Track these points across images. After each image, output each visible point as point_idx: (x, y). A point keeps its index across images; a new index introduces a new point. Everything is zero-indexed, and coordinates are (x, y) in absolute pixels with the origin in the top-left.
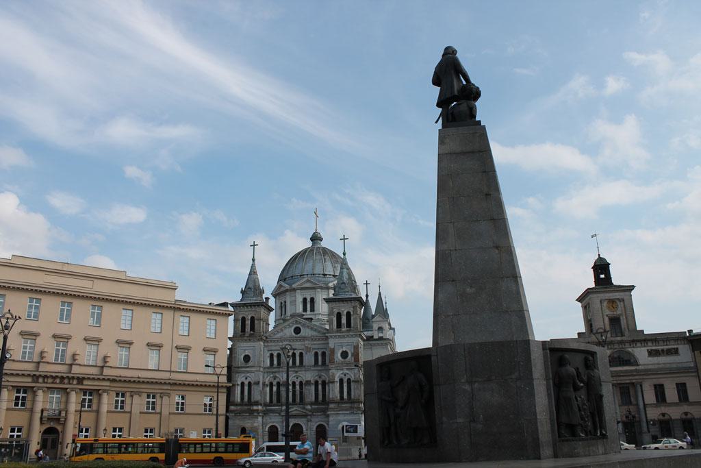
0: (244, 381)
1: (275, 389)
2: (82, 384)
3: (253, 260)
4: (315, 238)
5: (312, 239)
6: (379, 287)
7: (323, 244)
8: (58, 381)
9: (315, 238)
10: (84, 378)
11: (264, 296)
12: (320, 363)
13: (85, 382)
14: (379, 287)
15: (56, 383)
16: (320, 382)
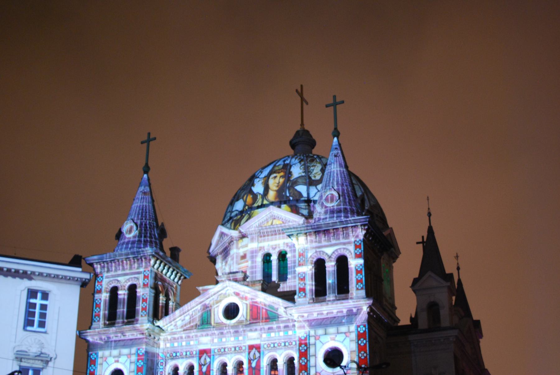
3: (146, 170)
6: (429, 215)
14: (429, 215)
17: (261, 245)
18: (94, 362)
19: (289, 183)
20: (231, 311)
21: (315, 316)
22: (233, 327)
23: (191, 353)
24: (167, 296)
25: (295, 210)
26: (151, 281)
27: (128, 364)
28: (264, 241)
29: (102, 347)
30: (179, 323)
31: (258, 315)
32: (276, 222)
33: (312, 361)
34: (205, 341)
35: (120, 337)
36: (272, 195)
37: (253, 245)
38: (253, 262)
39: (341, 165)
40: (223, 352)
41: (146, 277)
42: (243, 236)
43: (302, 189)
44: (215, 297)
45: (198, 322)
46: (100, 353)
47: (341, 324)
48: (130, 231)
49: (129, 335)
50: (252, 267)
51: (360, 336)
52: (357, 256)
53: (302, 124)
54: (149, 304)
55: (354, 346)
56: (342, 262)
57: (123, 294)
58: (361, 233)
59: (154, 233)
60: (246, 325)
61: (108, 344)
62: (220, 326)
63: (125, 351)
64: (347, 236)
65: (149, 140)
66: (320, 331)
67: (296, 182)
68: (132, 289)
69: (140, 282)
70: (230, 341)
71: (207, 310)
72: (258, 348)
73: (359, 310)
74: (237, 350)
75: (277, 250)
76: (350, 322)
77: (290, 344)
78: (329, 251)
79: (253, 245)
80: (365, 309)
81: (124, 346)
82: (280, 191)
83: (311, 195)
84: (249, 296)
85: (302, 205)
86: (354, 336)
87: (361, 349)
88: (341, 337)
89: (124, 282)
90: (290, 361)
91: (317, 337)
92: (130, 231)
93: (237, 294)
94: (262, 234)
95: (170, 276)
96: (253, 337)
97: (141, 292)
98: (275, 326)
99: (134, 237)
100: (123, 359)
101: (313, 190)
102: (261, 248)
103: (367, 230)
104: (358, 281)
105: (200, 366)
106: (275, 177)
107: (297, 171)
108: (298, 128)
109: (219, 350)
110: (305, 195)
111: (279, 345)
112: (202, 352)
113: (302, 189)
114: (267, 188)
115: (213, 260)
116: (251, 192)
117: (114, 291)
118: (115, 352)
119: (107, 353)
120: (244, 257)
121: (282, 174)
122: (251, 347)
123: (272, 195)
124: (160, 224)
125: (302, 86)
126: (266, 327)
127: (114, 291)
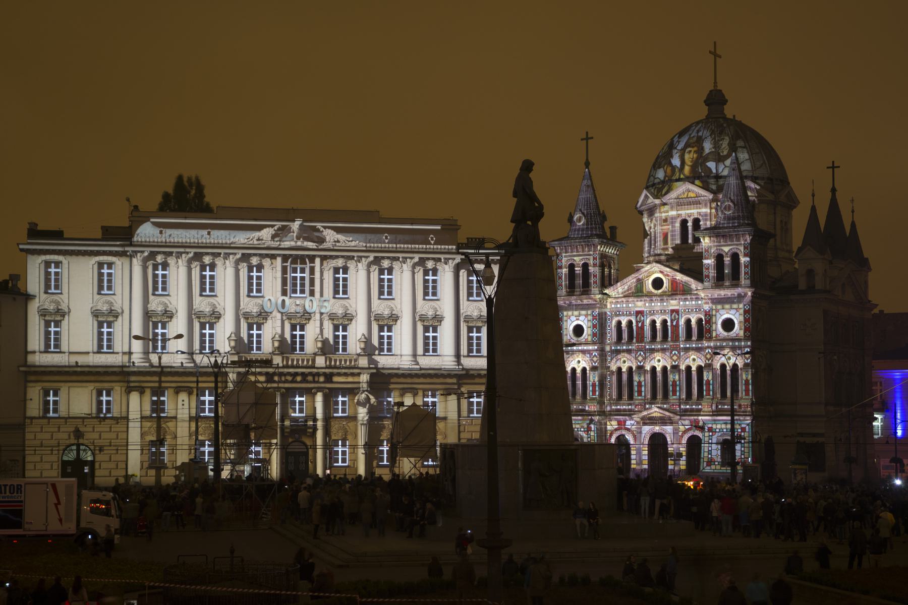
0: (576, 366)
1: (625, 377)
2: (332, 382)
3: (587, 164)
4: (716, 100)
5: (707, 102)
7: (729, 111)
8: (299, 378)
9: (716, 100)
10: (332, 375)
11: (607, 225)
13: (335, 379)
15: (296, 382)
17: (680, 212)
18: (561, 319)
19: (701, 160)
20: (658, 283)
21: (716, 296)
22: (660, 296)
23: (630, 313)
24: (610, 268)
25: (706, 187)
26: (598, 262)
27: (586, 321)
28: (682, 209)
29: (567, 309)
30: (620, 290)
31: (678, 290)
32: (692, 195)
33: (714, 326)
34: (640, 305)
35: (579, 302)
36: (687, 169)
37: (673, 213)
38: (673, 227)
39: (737, 179)
40: (652, 313)
41: (595, 259)
42: (665, 204)
43: (711, 165)
44: (646, 274)
45: (633, 290)
46: (565, 313)
47: (733, 303)
48: (580, 220)
49: (585, 302)
50: (672, 231)
51: (745, 312)
52: (745, 255)
53: (715, 82)
54: (598, 279)
55: (742, 318)
56: (735, 257)
57: (578, 270)
58: (748, 239)
59: (600, 228)
60: (669, 296)
61: (570, 307)
62: (650, 295)
63: (583, 312)
64: (738, 240)
65: (587, 139)
66: (719, 307)
67: (707, 159)
68: (585, 266)
69: (591, 262)
70: (657, 305)
71: (640, 282)
72: (677, 311)
73: (746, 295)
74: (663, 312)
75: (692, 218)
76: (739, 302)
77: (700, 310)
78: (726, 249)
79: (673, 213)
80: (750, 294)
81: (583, 309)
82: (693, 168)
83: (720, 170)
85: (712, 181)
86: (742, 311)
87: (746, 320)
88: (733, 312)
89: (578, 260)
90: (699, 321)
91: (717, 311)
92: (580, 220)
93: (661, 272)
94: (681, 203)
95: (611, 251)
96: (673, 304)
97: (591, 269)
98: (689, 297)
100: (582, 318)
101: (721, 167)
102: (679, 215)
103: (754, 236)
104: (745, 273)
105: (637, 322)
106: (690, 152)
107: (708, 146)
109: (650, 312)
110: (714, 171)
111: (692, 310)
112: (638, 313)
113: (711, 165)
114: (683, 163)
115: (641, 213)
116: (670, 164)
117: (572, 267)
118: (576, 313)
119: (570, 313)
120: (665, 220)
121: (695, 149)
122: (672, 311)
123: (687, 169)
125: (715, 43)
126: (683, 297)
127: (572, 267)
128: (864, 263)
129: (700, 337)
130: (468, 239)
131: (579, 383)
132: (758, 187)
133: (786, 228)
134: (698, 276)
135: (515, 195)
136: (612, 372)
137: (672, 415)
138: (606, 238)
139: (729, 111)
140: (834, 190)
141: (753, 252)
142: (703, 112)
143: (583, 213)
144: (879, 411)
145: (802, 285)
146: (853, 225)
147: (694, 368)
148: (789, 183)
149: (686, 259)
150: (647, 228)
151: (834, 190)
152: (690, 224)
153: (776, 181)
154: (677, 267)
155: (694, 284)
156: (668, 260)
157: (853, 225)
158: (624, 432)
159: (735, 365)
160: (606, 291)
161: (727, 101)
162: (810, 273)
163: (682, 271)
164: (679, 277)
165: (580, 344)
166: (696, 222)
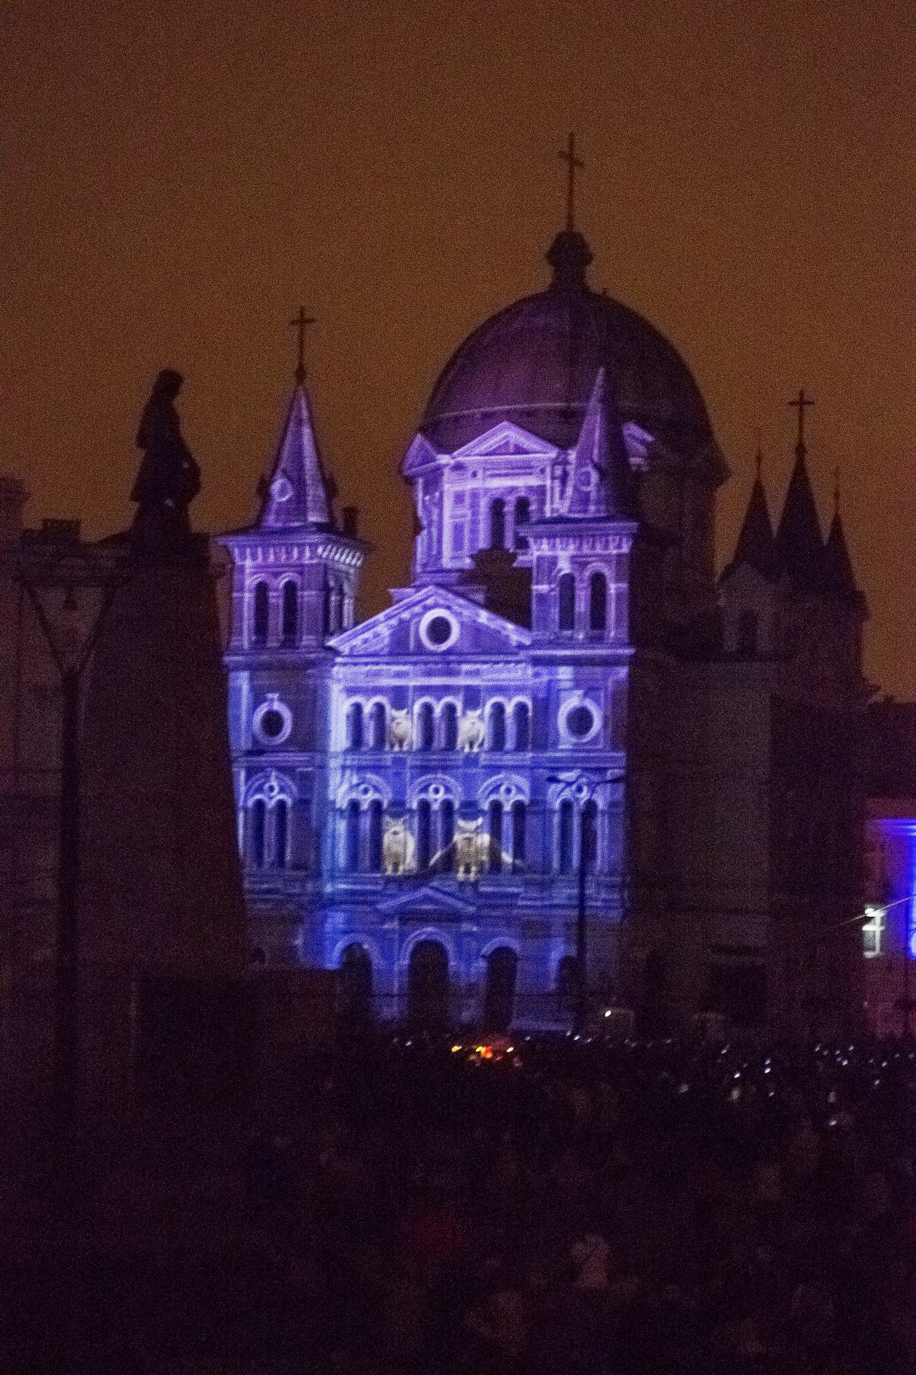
3: (300, 374)
4: (569, 253)
6: (759, 459)
7: (596, 278)
9: (569, 253)
11: (339, 504)
12: (510, 745)
14: (759, 459)
16: (507, 808)
53: (570, 218)
56: (598, 581)
65: (303, 321)
84: (462, 615)
90: (521, 709)
99: (288, 501)
108: (562, 227)
115: (410, 482)
117: (262, 590)
124: (327, 473)
128: (855, 602)
129: (521, 746)
130: (45, 521)
131: (270, 834)
132: (650, 438)
133: (704, 523)
134: (521, 615)
135: (142, 441)
136: (341, 811)
137: (460, 905)
138: (336, 533)
139: (596, 278)
140: (800, 450)
141: (636, 568)
142: (540, 278)
143: (289, 478)
144: (878, 902)
145: (731, 644)
146: (837, 522)
147: (507, 808)
148: (710, 433)
149: (499, 582)
150: (420, 512)
151: (800, 450)
152: (509, 509)
153: (687, 430)
154: (480, 597)
155: (512, 632)
156: (461, 582)
157: (837, 522)
158: (359, 937)
159: (591, 805)
160: (332, 643)
161: (591, 259)
162: (748, 621)
163: (491, 605)
164: (483, 617)
165: (276, 750)
166: (522, 505)
